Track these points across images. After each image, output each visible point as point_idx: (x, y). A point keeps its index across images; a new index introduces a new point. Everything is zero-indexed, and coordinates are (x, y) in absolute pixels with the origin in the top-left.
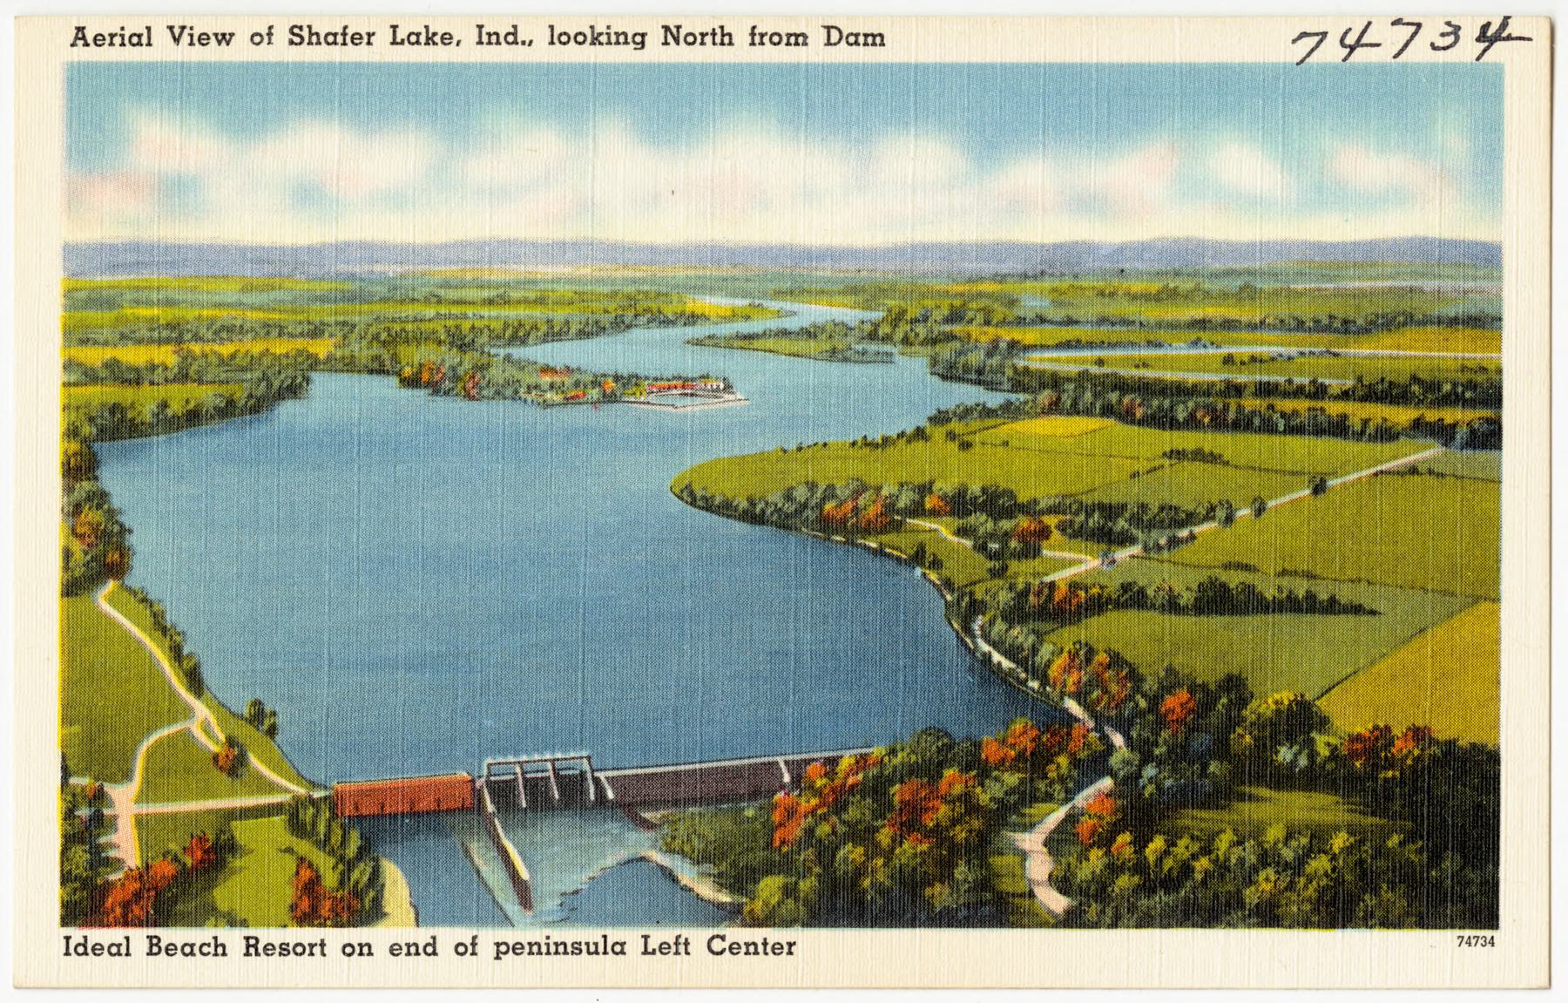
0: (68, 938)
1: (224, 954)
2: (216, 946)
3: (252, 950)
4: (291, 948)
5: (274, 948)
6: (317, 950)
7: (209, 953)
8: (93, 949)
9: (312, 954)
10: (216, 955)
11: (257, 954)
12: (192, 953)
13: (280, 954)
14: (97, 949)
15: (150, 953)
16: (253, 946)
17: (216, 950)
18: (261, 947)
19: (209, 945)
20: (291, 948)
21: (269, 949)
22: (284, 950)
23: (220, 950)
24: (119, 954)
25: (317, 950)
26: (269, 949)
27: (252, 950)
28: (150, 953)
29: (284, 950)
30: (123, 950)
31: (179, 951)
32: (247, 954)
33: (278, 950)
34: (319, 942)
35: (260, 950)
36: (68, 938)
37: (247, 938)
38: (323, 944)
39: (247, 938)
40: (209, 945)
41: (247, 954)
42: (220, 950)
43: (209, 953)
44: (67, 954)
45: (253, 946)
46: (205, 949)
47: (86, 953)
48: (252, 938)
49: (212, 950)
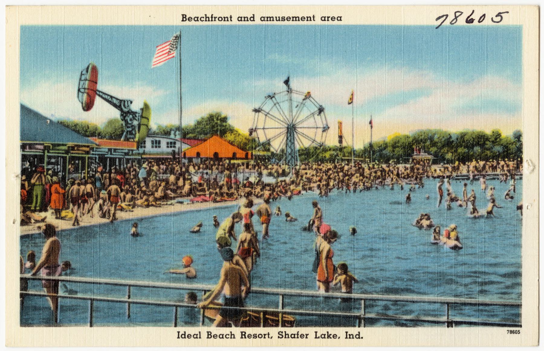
0: (179, 332)
1: (234, 338)
2: (231, 335)
3: (243, 336)
4: (257, 336)
5: (251, 336)
6: (267, 336)
7: (228, 338)
8: (188, 336)
9: (265, 338)
10: (231, 338)
11: (245, 338)
12: (223, 338)
13: (254, 338)
14: (189, 336)
15: (208, 338)
16: (244, 335)
17: (231, 336)
18: (246, 335)
19: (229, 335)
20: (257, 336)
21: (250, 336)
22: (255, 336)
23: (233, 336)
24: (197, 338)
25: (267, 336)
26: (250, 336)
27: (243, 336)
28: (208, 338)
29: (255, 336)
30: (198, 336)
31: (218, 337)
32: (242, 338)
33: (253, 336)
34: (267, 333)
35: (247, 336)
36: (179, 332)
37: (242, 332)
38: (269, 334)
39: (242, 332)
40: (229, 335)
41: (242, 338)
42: (233, 336)
43: (228, 338)
44: (178, 338)
45: (244, 335)
46: (227, 336)
47: (185, 338)
48: (244, 332)
49: (230, 336)
